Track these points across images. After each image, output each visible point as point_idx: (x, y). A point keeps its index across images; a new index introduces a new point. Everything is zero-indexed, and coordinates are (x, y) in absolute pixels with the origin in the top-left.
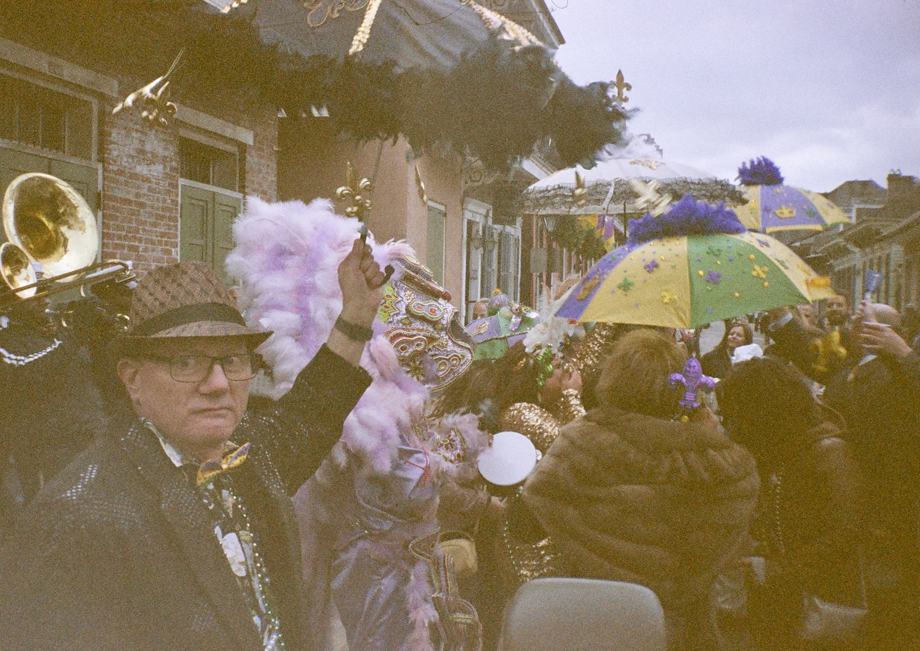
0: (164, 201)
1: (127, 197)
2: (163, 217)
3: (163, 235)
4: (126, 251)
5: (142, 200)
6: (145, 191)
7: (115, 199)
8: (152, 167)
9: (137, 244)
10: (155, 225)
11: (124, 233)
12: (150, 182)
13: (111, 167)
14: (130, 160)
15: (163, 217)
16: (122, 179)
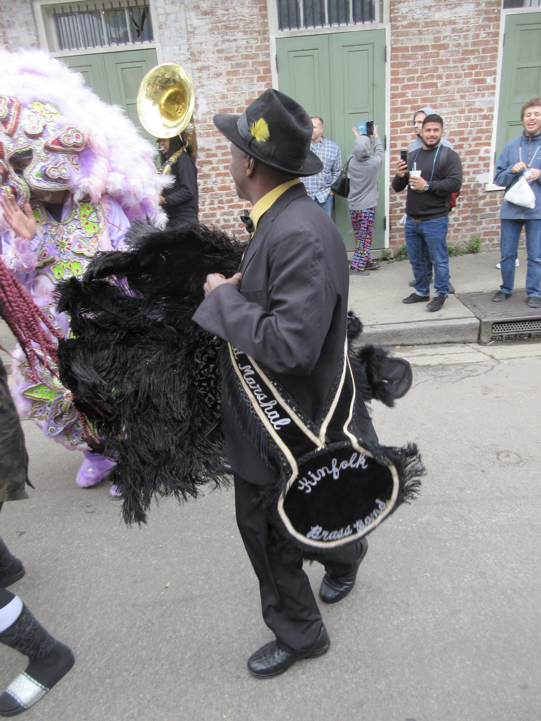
0: (477, 36)
1: (420, 44)
2: (472, 52)
3: (472, 68)
4: (420, 89)
5: (442, 42)
6: (448, 33)
7: (406, 49)
8: (458, 9)
9: (435, 81)
10: (462, 60)
11: (416, 75)
12: (455, 23)
13: (399, 24)
14: (426, 11)
15: (472, 52)
16: (414, 30)
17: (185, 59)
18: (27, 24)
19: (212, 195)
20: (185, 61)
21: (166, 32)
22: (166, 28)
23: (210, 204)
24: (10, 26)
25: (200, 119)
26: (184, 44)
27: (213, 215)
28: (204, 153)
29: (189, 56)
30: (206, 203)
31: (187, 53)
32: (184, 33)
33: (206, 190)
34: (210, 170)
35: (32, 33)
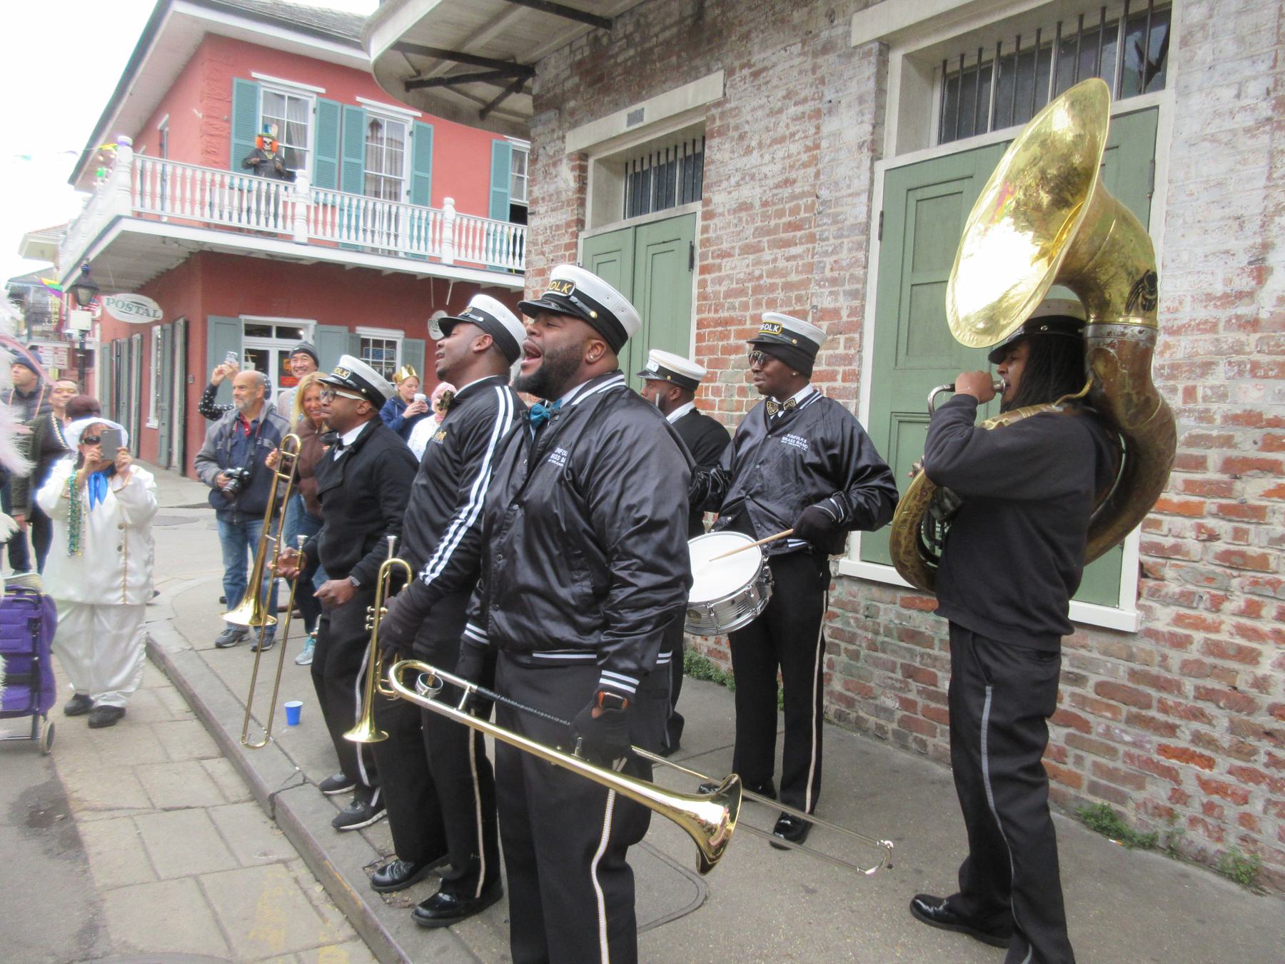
17: (1250, 123)
18: (861, 100)
19: (1255, 583)
20: (1247, 131)
21: (1203, 52)
22: (1206, 38)
23: (1242, 613)
24: (833, 107)
25: (1264, 315)
26: (1255, 78)
27: (1250, 657)
28: (1258, 434)
29: (1270, 113)
30: (1227, 606)
31: (1264, 104)
32: (1265, 42)
33: (1233, 559)
34: (1268, 494)
35: (868, 117)
